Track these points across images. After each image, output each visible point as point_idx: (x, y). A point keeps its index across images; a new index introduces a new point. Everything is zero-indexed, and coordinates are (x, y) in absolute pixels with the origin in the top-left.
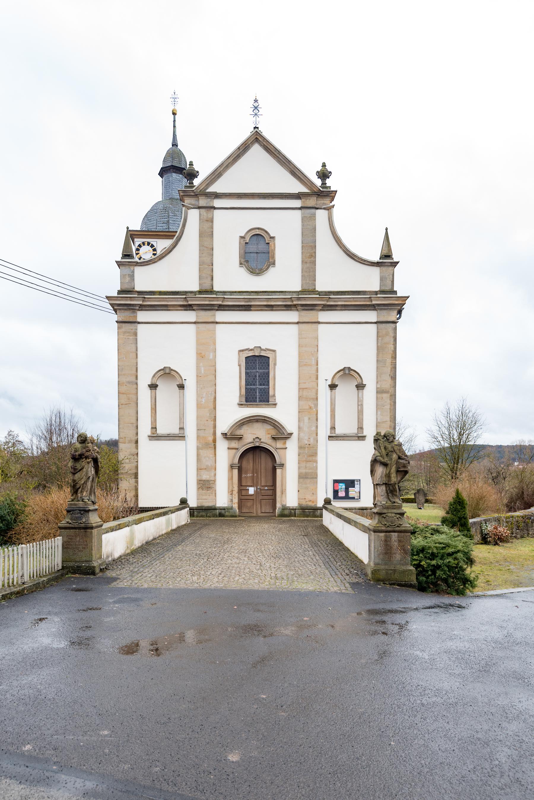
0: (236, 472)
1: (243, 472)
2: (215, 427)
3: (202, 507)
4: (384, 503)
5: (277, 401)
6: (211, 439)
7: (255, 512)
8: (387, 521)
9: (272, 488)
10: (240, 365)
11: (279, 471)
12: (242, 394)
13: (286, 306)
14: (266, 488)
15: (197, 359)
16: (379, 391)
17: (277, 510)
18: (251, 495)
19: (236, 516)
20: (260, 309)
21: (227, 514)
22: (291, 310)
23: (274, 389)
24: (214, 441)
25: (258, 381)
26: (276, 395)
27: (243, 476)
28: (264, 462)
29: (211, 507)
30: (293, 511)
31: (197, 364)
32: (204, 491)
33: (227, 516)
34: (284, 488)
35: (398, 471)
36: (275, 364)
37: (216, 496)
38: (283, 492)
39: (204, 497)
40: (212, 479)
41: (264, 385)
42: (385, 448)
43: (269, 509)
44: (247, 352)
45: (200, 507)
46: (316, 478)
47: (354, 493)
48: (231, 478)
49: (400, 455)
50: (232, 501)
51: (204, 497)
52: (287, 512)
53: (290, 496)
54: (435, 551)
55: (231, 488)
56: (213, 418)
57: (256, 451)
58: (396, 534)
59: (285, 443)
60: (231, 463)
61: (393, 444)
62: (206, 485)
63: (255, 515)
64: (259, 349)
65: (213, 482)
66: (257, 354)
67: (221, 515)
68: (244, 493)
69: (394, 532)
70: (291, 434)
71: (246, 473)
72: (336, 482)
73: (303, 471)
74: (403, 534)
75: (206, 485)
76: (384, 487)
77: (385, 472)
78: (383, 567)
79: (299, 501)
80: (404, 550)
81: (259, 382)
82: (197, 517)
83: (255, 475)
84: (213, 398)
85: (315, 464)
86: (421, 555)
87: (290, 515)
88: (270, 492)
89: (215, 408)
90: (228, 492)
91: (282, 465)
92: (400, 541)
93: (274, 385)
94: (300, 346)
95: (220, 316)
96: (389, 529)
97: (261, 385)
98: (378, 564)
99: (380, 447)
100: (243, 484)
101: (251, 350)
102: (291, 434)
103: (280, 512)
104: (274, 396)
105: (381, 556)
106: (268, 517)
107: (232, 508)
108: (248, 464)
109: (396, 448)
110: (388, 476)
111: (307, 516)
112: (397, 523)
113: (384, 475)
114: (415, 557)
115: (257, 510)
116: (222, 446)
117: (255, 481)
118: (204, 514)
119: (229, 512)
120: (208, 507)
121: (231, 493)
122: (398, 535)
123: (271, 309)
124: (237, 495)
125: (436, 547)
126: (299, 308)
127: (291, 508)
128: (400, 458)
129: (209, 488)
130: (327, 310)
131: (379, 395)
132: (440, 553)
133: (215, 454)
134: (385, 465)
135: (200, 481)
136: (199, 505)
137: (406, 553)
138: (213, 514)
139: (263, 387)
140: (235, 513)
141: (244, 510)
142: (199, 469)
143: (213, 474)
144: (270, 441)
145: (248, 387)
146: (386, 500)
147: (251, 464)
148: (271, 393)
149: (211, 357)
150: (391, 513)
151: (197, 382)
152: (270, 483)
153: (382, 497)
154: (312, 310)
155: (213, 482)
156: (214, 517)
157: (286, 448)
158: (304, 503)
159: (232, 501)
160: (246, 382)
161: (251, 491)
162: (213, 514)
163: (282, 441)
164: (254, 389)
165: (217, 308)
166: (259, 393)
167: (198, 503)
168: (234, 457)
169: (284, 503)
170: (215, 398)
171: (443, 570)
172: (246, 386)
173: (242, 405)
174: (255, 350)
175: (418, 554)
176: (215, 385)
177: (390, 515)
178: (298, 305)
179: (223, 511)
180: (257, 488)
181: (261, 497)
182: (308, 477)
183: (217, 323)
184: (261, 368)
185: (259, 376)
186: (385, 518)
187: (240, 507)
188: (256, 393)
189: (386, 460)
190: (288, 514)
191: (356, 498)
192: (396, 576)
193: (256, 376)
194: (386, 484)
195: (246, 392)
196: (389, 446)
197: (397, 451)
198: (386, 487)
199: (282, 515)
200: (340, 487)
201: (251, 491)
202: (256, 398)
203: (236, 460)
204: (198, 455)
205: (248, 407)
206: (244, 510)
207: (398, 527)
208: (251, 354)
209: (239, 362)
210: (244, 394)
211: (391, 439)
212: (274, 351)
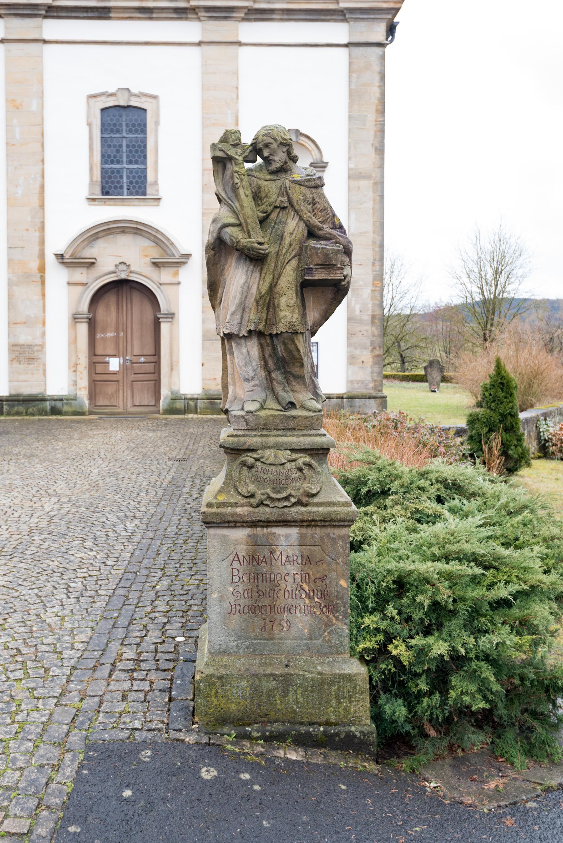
0: (83, 329)
1: (98, 329)
2: (42, 242)
3: (18, 395)
4: (251, 407)
5: (161, 194)
6: (34, 265)
7: (121, 405)
8: (258, 480)
9: (152, 359)
10: (89, 125)
11: (164, 327)
12: (95, 179)
13: (177, 10)
14: (142, 359)
15: (7, 111)
16: (354, 176)
17: (161, 401)
18: (115, 373)
19: (83, 414)
20: (127, 15)
21: (66, 408)
22: (187, 19)
23: (156, 170)
24: (42, 269)
25: (125, 155)
26: (160, 182)
27: (99, 336)
28: (138, 309)
30: (192, 403)
31: (7, 120)
33: (66, 414)
34: (175, 359)
35: (305, 286)
36: (157, 123)
37: (45, 375)
39: (23, 377)
40: (38, 341)
41: (136, 162)
42: (257, 196)
43: (147, 399)
44: (103, 98)
45: (14, 396)
48: (73, 341)
49: (315, 221)
50: (75, 383)
51: (23, 377)
52: (180, 405)
54: (445, 595)
56: (39, 225)
57: (121, 288)
58: (294, 532)
59: (176, 274)
60: (74, 312)
61: (286, 180)
63: (121, 410)
64: (126, 94)
65: (40, 348)
66: (122, 103)
67: (55, 411)
69: (285, 523)
70: (188, 256)
71: (104, 331)
74: (319, 532)
75: (25, 354)
76: (252, 348)
77: (254, 290)
78: (240, 665)
79: (204, 384)
80: (324, 595)
81: (128, 156)
82: (8, 414)
83: (122, 334)
84: (38, 185)
86: (391, 610)
87: (185, 411)
89: (42, 206)
90: (69, 368)
91: (171, 316)
92: (307, 560)
93: (156, 162)
94: (205, 88)
95: (53, 28)
96: (265, 513)
97: (130, 162)
98: (224, 652)
99: (235, 189)
100: (99, 351)
101: (112, 95)
102: (188, 256)
103: (169, 405)
104: (156, 183)
105: (236, 621)
106: (146, 413)
107: (75, 398)
108: (108, 313)
109: (297, 194)
110: (268, 302)
112: (295, 489)
113: (251, 302)
114: (369, 621)
115: (124, 400)
116: (57, 278)
117: (121, 346)
118: (21, 409)
119: (70, 405)
120: (30, 395)
121: (74, 368)
122: (302, 536)
123: (148, 15)
125: (449, 576)
126: (202, 14)
127: (189, 397)
128: (312, 233)
129: (31, 360)
130: (256, 20)
131: (354, 183)
132: (463, 599)
133: (43, 295)
134: (255, 259)
135: (14, 345)
136: (13, 393)
137: (333, 608)
138: (39, 410)
139: (136, 166)
140: (81, 406)
142: (12, 324)
143: (38, 333)
144: (149, 271)
145: (107, 166)
146: (260, 395)
147: (114, 314)
148: (150, 178)
149: (34, 107)
150: (278, 447)
151: (7, 155)
152: (150, 350)
153: (248, 386)
154: (226, 18)
155: (40, 348)
156: (40, 414)
157: (179, 283)
159: (75, 383)
160: (103, 156)
161: (114, 364)
162: (39, 410)
163: (171, 270)
164: (119, 171)
165: (43, 12)
166: (128, 177)
167: (10, 388)
168: (79, 301)
169: (175, 388)
170: (42, 187)
171: (473, 675)
172: (102, 164)
173: (94, 200)
174: (119, 94)
175: (380, 607)
176: (43, 161)
177: (270, 455)
178: (198, 7)
179: (59, 404)
180: (125, 360)
181: (132, 377)
183: (45, 42)
184: (130, 131)
185: (128, 146)
186: (251, 467)
188: (121, 177)
189: (256, 238)
190: (182, 407)
192: (295, 701)
193: (121, 146)
194: (260, 334)
195: (103, 177)
196: (271, 188)
197: (304, 208)
198: (262, 347)
199: (171, 411)
201: (114, 364)
202: (122, 187)
203: (84, 307)
204: (10, 296)
205: (105, 204)
206: (101, 401)
207: (299, 503)
208: (111, 102)
209: (88, 117)
210: (99, 179)
211: (280, 157)
212: (155, 97)
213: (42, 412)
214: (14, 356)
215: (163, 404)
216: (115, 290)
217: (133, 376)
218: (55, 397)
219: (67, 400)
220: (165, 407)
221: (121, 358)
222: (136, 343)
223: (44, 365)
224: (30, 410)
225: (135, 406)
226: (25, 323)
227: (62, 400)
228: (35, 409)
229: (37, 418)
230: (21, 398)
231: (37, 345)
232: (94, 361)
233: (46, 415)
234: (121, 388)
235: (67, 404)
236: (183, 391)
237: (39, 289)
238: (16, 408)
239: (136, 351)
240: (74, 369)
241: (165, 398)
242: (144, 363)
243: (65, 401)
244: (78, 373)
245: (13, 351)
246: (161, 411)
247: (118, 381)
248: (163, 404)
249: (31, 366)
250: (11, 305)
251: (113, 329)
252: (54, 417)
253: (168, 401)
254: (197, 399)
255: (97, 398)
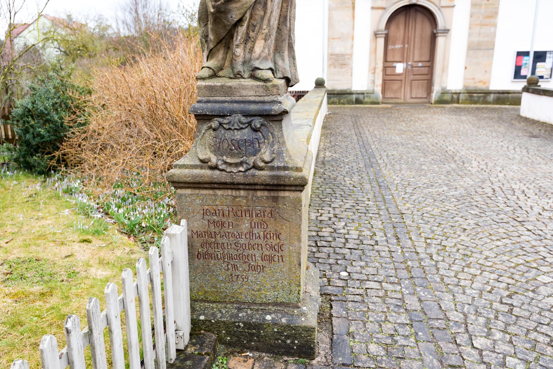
0: (381, 41)
1: (390, 42)
3: (333, 90)
7: (402, 97)
9: (428, 64)
11: (440, 41)
14: (420, 64)
18: (399, 75)
19: (378, 103)
21: (366, 100)
27: (390, 47)
28: (420, 27)
29: (346, 91)
32: (336, 70)
33: (366, 103)
38: (444, 69)
40: (348, 52)
43: (421, 93)
45: (331, 91)
46: (493, 49)
47: (543, 70)
50: (374, 82)
52: (447, 97)
53: (452, 76)
55: (373, 65)
60: (375, 29)
62: (339, 61)
63: (402, 101)
65: (349, 56)
67: (358, 102)
68: (389, 71)
71: (394, 43)
72: (521, 54)
73: (475, 39)
75: (339, 61)
83: (406, 46)
85: (493, 29)
87: (452, 101)
88: (425, 71)
90: (369, 70)
100: (389, 59)
103: (439, 97)
107: (373, 93)
108: (398, 31)
111: (475, 103)
115: (406, 94)
118: (336, 100)
119: (369, 97)
120: (341, 91)
124: (381, 74)
127: (453, 91)
129: (343, 65)
133: (354, 17)
135: (332, 55)
140: (377, 98)
141: (388, 95)
142: (331, 39)
152: (426, 57)
155: (349, 56)
156: (349, 103)
157: (454, 6)
158: (472, 85)
161: (400, 68)
162: (348, 101)
169: (444, 85)
179: (361, 97)
180: (407, 65)
181: (412, 77)
182: (481, 47)
187: (384, 91)
190: (448, 100)
191: (545, 77)
199: (441, 102)
200: (524, 62)
201: (400, 68)
204: (330, 19)
206: (388, 95)
213: (350, 102)
214: (331, 62)
215: (434, 96)
216: (404, 12)
217: (412, 76)
218: (359, 92)
219: (367, 93)
220: (437, 99)
221: (405, 64)
222: (417, 52)
223: (352, 69)
224: (342, 101)
225: (412, 98)
226: (340, 38)
227: (363, 94)
228: (345, 100)
229: (346, 106)
230: (336, 92)
231: (347, 55)
232: (386, 66)
233: (352, 104)
234: (403, 85)
235: (367, 96)
236: (448, 88)
237: (351, 11)
238: (332, 99)
239: (416, 59)
240: (373, 71)
241: (437, 93)
242: (421, 67)
243: (366, 95)
244: (376, 75)
245: (331, 59)
246: (433, 101)
247: (401, 80)
248: (434, 96)
249: (343, 70)
250: (331, 25)
251: (401, 42)
252: (358, 106)
253: (439, 94)
254: (460, 93)
255: (386, 91)
